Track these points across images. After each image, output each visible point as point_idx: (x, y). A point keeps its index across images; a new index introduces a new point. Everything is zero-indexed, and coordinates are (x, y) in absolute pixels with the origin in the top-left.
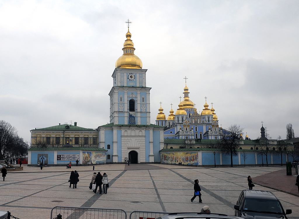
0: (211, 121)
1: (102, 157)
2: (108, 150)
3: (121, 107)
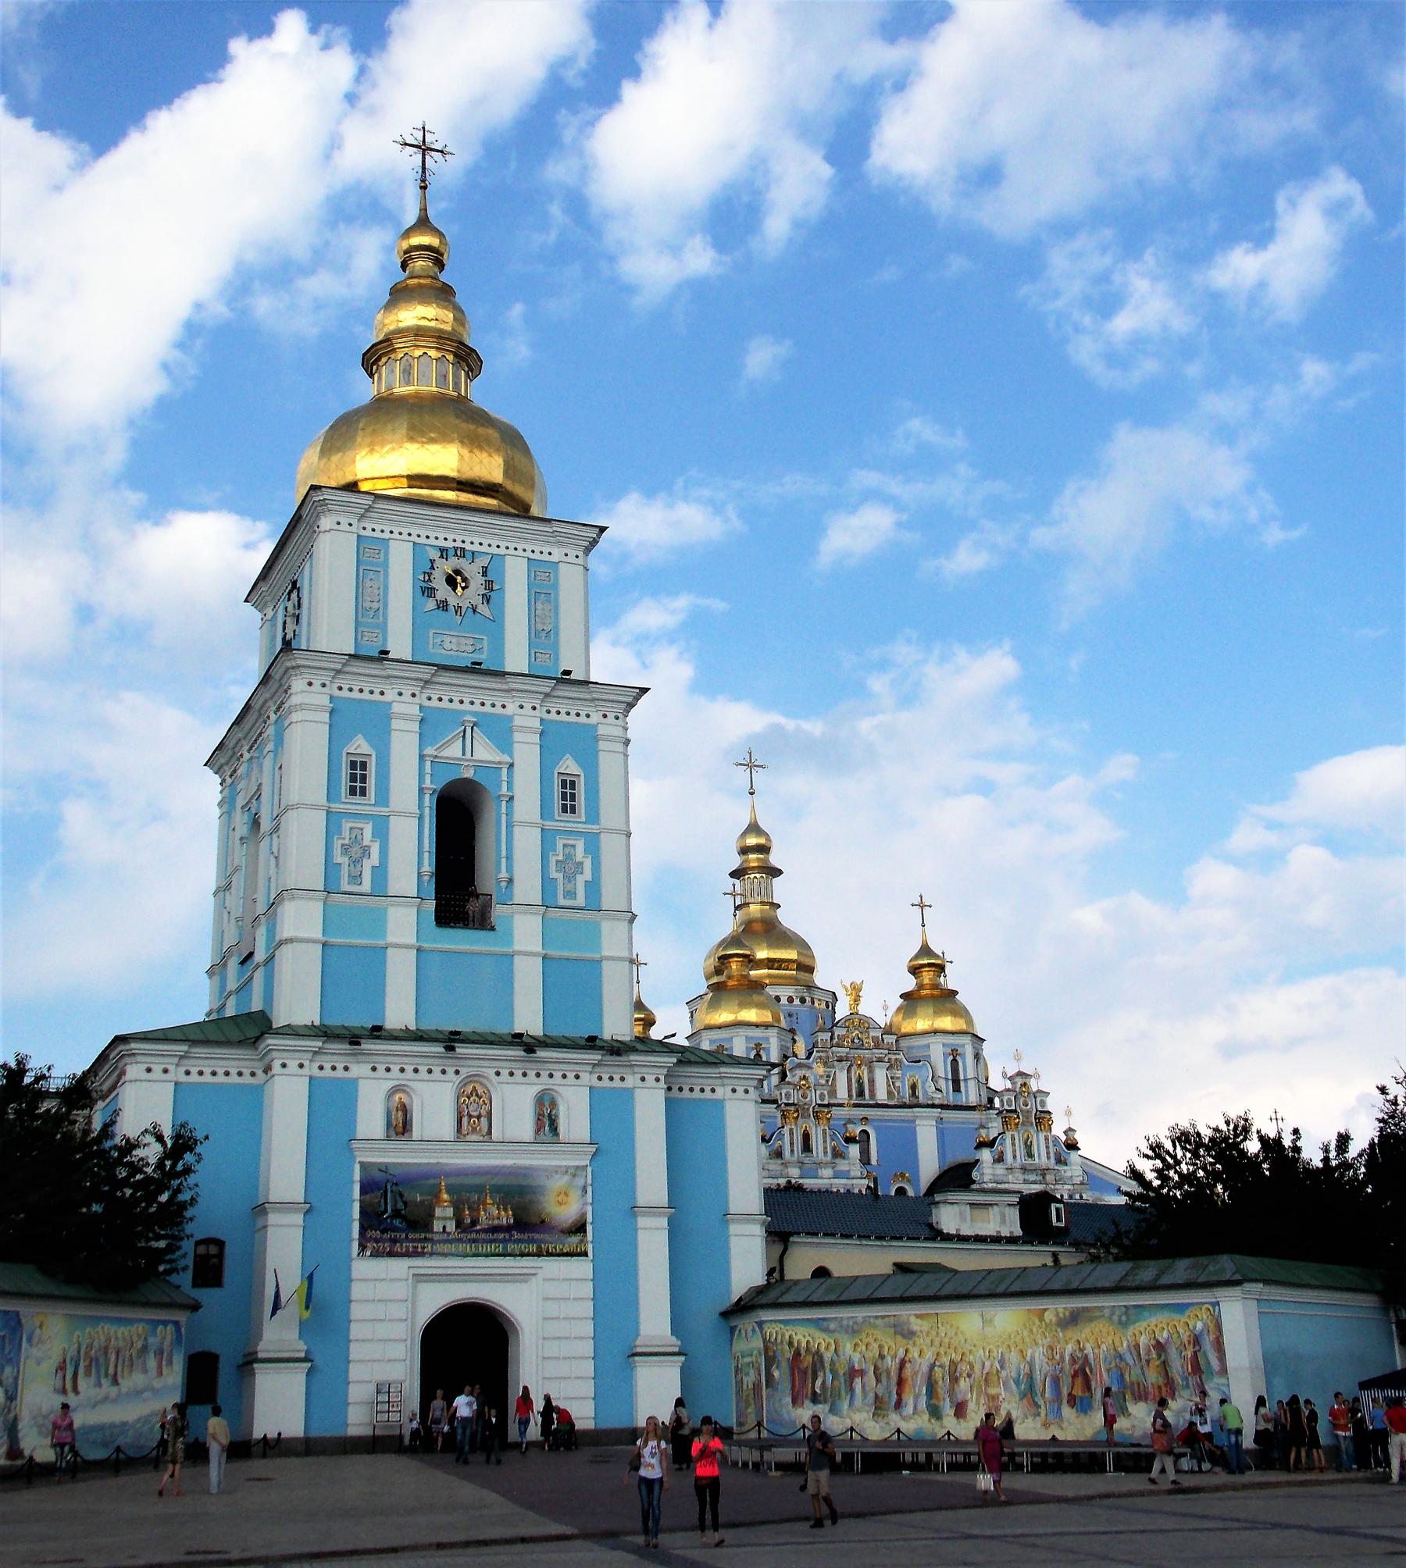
0: (972, 1084)
1: (137, 1379)
2: (205, 1295)
3: (356, 851)
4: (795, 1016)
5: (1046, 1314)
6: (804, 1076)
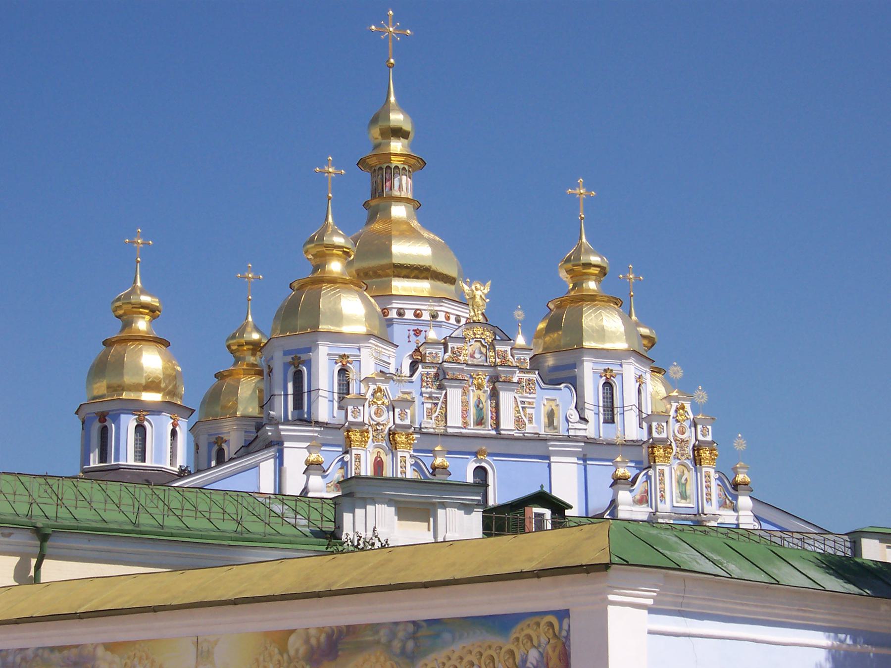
4: (423, 333)
5: (292, 639)
6: (379, 390)
